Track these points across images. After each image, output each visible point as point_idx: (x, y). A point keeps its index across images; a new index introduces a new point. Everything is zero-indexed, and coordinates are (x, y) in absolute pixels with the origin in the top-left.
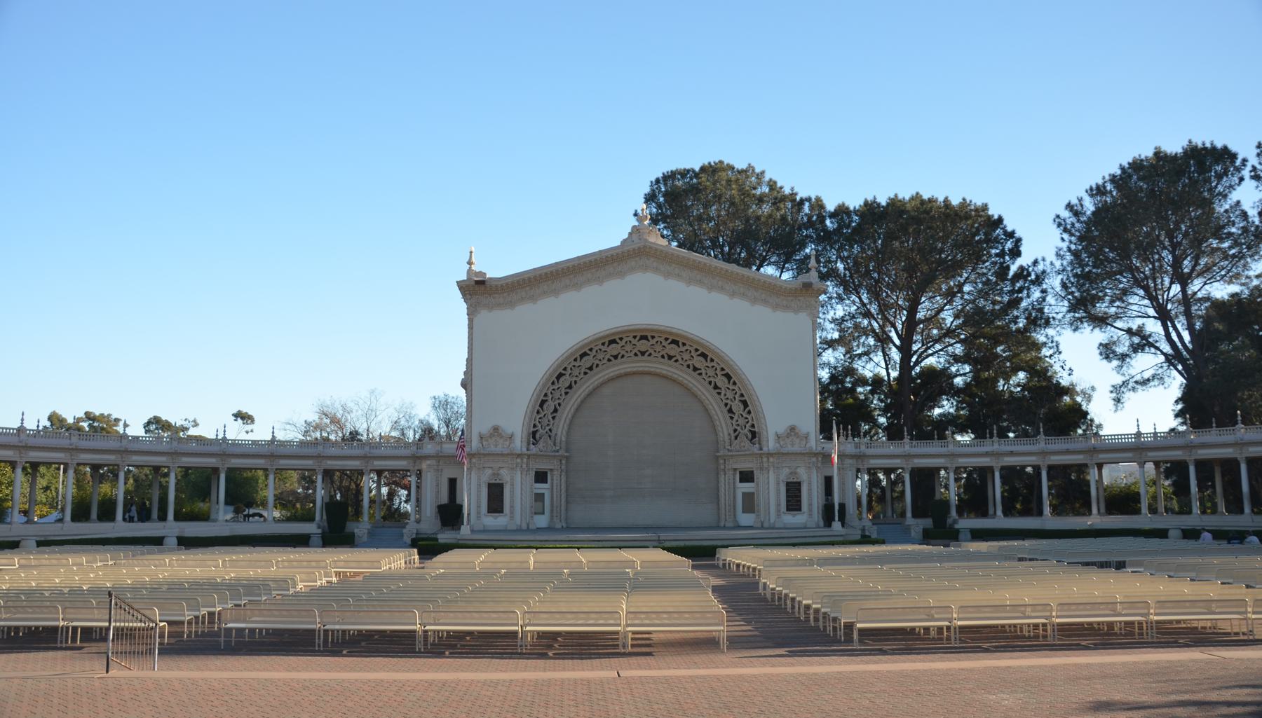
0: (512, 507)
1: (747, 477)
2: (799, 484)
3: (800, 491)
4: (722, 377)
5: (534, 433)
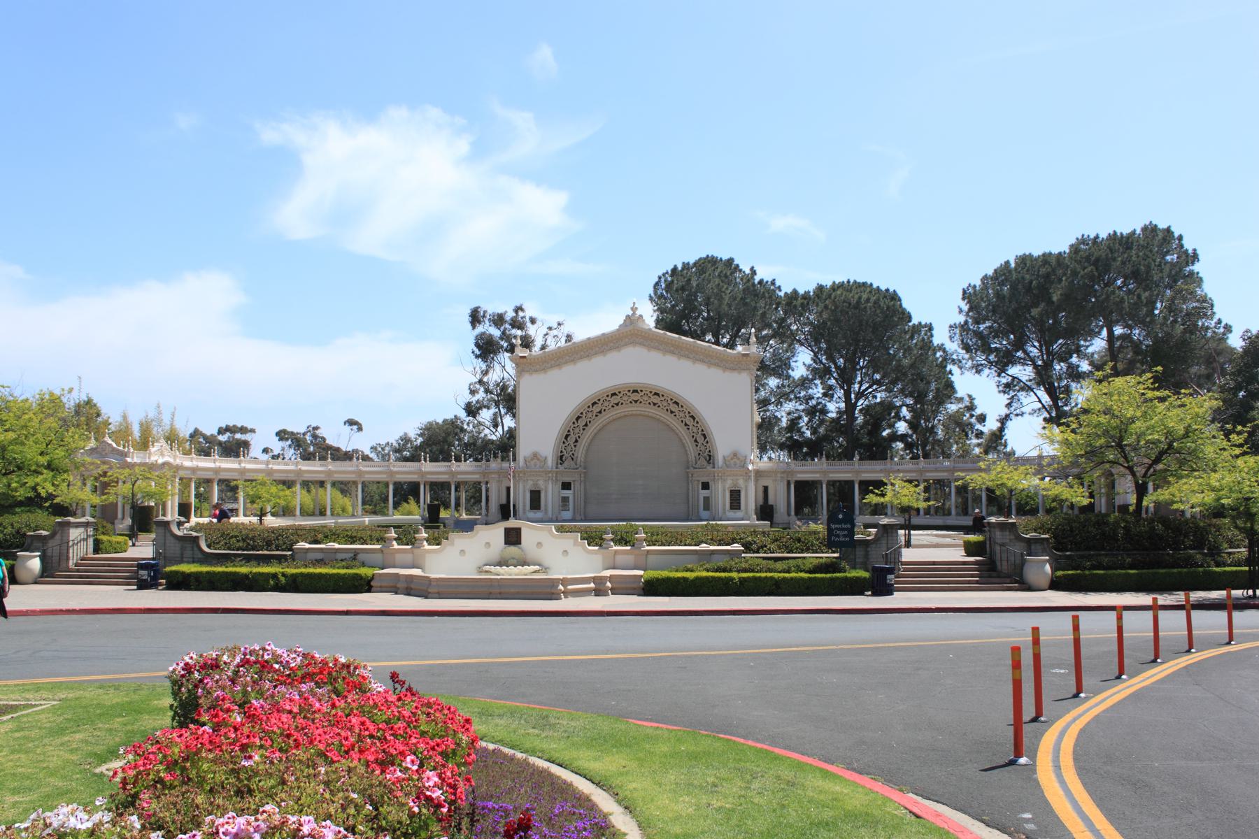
1: (706, 486)
4: (692, 419)
5: (561, 457)
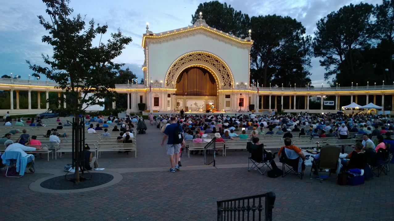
0: (162, 105)
2: (243, 99)
3: (243, 101)
